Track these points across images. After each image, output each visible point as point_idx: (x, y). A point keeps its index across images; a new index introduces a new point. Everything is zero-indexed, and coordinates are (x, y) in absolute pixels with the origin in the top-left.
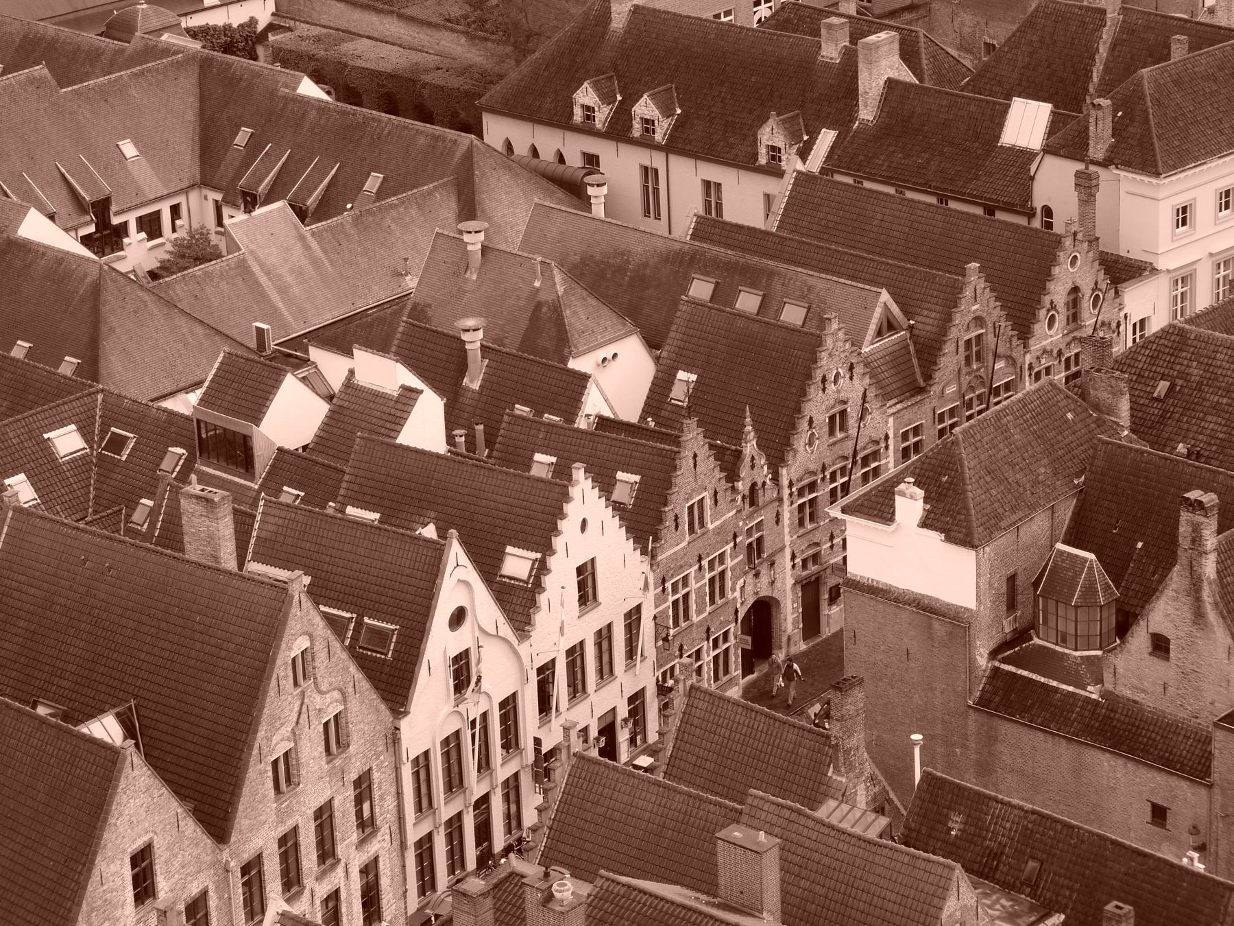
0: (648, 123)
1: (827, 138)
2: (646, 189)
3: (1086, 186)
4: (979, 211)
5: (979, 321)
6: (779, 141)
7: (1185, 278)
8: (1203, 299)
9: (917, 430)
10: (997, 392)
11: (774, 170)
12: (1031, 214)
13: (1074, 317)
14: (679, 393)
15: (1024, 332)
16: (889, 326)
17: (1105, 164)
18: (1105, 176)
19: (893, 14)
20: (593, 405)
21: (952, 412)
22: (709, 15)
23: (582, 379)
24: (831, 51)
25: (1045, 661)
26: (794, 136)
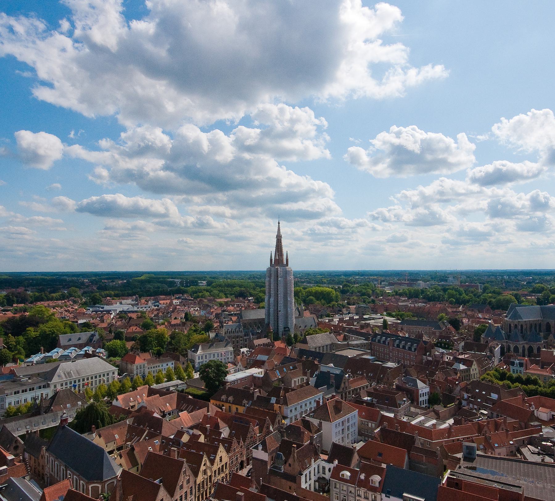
0: (230, 401)
7: (291, 418)
11: (244, 406)
13: (279, 424)
20: (222, 436)
23: (221, 432)
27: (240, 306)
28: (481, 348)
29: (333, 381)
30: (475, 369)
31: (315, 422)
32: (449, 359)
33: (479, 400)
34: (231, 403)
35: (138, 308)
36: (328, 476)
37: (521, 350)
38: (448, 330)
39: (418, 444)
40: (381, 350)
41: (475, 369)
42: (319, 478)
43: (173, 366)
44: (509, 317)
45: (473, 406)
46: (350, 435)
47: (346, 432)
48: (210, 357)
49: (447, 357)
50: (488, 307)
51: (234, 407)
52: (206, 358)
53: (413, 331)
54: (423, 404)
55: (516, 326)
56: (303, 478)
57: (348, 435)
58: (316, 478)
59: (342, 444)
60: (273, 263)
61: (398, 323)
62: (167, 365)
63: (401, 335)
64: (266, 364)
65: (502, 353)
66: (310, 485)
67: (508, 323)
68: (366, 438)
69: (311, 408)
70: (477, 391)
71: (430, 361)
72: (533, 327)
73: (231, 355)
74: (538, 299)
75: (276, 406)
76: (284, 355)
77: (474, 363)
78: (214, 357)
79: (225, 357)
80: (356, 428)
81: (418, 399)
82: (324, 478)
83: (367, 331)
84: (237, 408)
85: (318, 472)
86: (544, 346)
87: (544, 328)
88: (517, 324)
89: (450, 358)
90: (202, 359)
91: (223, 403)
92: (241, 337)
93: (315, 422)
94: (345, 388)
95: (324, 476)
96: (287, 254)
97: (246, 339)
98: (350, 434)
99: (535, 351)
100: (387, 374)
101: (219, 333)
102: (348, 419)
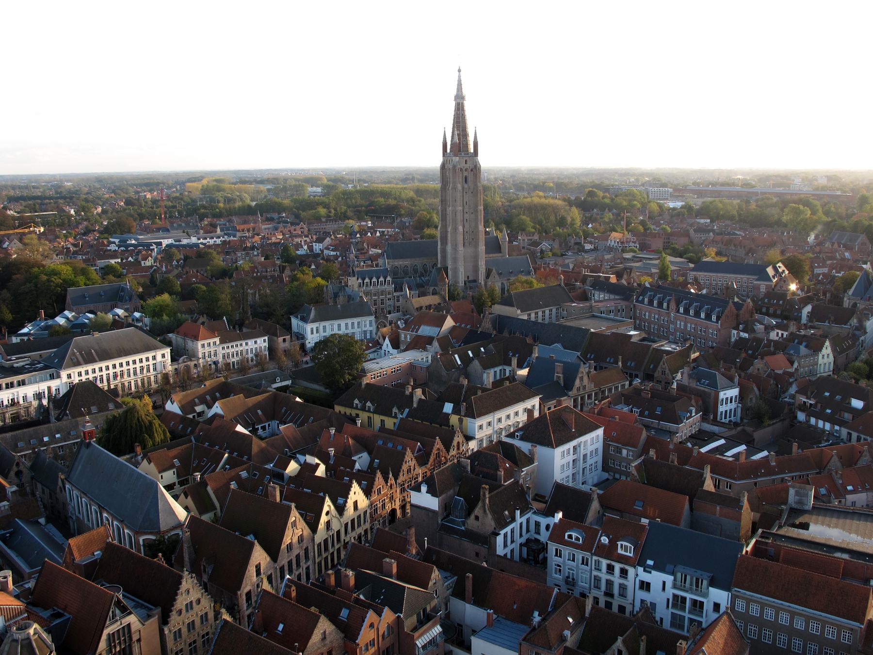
1: (407, 410)
3: (461, 421)
4: (438, 426)
5: (438, 449)
6: (397, 411)
7: (482, 440)
11: (396, 417)
12: (449, 427)
14: (375, 465)
15: (448, 451)
17: (465, 416)
18: (464, 419)
19: (421, 385)
20: (357, 466)
22: (382, 385)
23: (355, 461)
24: (407, 393)
25: (453, 522)
26: (400, 410)
27: (386, 233)
29: (559, 375)
30: (828, 354)
31: (525, 446)
32: (780, 335)
33: (829, 411)
34: (372, 412)
35: (199, 239)
36: (544, 536)
39: (709, 485)
42: (528, 540)
43: (266, 344)
45: (817, 423)
46: (587, 471)
47: (581, 465)
48: (332, 330)
49: (778, 333)
51: (377, 419)
52: (325, 331)
53: (717, 284)
56: (500, 539)
57: (583, 469)
58: (523, 540)
60: (448, 151)
62: (256, 342)
63: (692, 291)
64: (436, 344)
66: (512, 551)
68: (617, 476)
70: (827, 394)
71: (745, 339)
73: (370, 326)
75: (454, 419)
77: (827, 343)
78: (339, 329)
80: (599, 458)
82: (537, 541)
84: (382, 421)
85: (528, 531)
89: (782, 335)
90: (317, 332)
92: (389, 293)
93: (525, 446)
94: (581, 388)
95: (537, 537)
96: (476, 133)
97: (398, 297)
100: (661, 363)
101: (347, 286)
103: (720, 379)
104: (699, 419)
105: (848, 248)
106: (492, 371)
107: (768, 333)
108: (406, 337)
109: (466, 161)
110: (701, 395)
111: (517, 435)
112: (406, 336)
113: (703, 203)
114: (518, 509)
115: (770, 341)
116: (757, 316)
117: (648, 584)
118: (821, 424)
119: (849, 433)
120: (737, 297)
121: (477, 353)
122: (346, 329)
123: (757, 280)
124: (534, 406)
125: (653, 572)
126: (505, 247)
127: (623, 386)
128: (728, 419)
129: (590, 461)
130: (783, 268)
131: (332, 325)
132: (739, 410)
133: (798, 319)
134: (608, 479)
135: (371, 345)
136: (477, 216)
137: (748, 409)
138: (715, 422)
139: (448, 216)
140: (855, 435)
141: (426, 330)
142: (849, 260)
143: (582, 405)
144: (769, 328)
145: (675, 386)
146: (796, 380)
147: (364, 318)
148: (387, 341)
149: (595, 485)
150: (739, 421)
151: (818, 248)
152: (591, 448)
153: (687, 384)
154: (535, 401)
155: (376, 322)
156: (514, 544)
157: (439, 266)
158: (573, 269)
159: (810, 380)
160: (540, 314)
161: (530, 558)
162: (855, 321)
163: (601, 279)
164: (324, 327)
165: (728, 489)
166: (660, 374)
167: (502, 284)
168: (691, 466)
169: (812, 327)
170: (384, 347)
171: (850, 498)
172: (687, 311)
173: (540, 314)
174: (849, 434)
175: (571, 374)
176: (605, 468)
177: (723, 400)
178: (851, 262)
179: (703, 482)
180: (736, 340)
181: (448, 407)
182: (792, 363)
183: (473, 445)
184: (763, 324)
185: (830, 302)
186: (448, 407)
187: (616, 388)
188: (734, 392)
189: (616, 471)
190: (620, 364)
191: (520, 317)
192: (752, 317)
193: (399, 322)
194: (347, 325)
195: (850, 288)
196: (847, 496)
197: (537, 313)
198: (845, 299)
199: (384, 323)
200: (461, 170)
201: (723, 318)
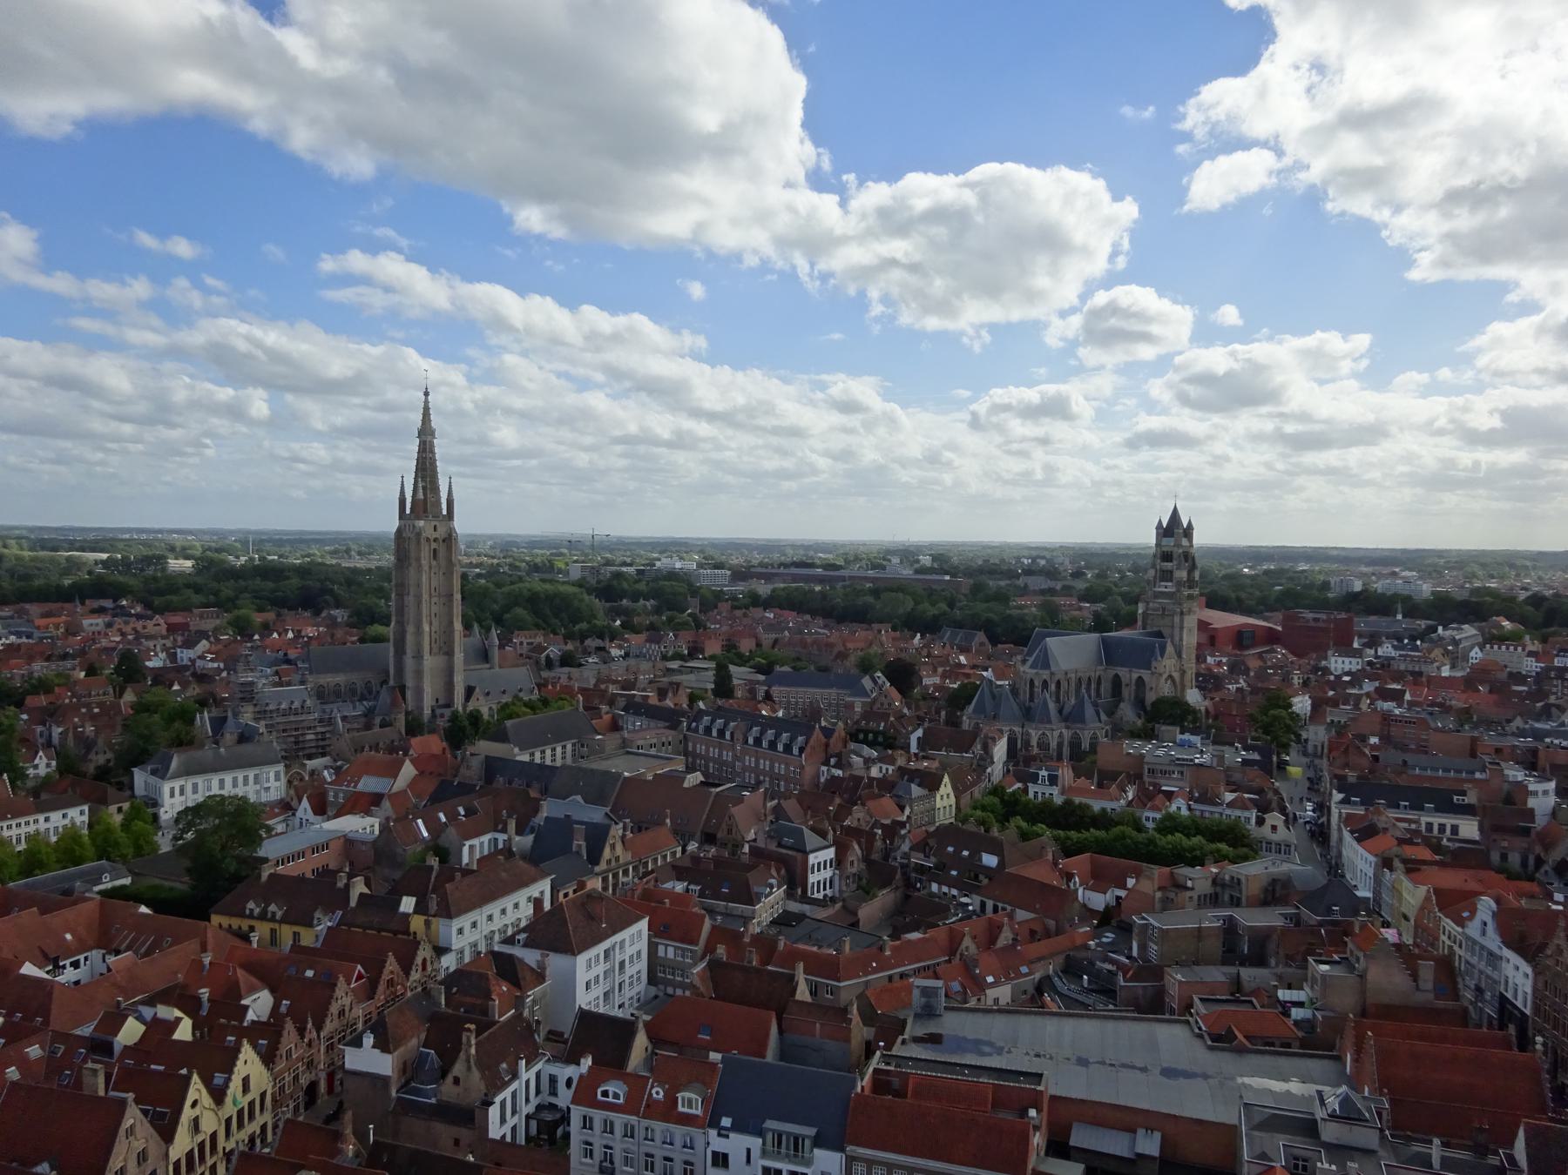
0: (274, 914)
2: (272, 936)
3: (427, 924)
5: (392, 972)
7: (462, 952)
8: (467, 960)
9: (370, 1013)
10: (398, 997)
12: (409, 934)
13: (424, 968)
14: (283, 1009)
16: (360, 977)
17: (434, 916)
18: (433, 920)
20: (251, 1016)
21: (382, 1006)
23: (246, 1008)
24: (340, 884)
25: (417, 1092)
28: (963, 742)
29: (580, 843)
30: (948, 795)
31: (530, 957)
32: (884, 771)
36: (564, 1098)
37: (1054, 744)
38: (886, 696)
39: (803, 993)
40: (714, 752)
41: (948, 795)
42: (539, 1108)
44: (1029, 664)
45: (940, 889)
48: (209, 789)
49: (881, 768)
50: (981, 636)
51: (286, 932)
53: (797, 703)
54: (818, 891)
55: (1045, 684)
56: (494, 1112)
57: (620, 984)
58: (531, 1109)
59: (601, 1010)
60: (408, 511)
61: (758, 682)
63: (764, 712)
64: (386, 804)
65: (1012, 752)
66: (514, 1129)
67: (1029, 677)
68: (670, 990)
69: (519, 920)
70: (950, 849)
71: (838, 777)
72: (1083, 686)
73: (277, 778)
74: (1097, 615)
75: (417, 923)
76: (440, 775)
77: (946, 779)
79: (258, 787)
80: (643, 965)
81: (806, 878)
82: (553, 1107)
83: (676, 705)
85: (538, 1092)
86: (1107, 731)
87: (1106, 687)
88: (1048, 680)
89: (887, 769)
91: (253, 923)
93: (530, 957)
94: (613, 860)
95: (553, 1100)
98: (627, 981)
99: (1085, 745)
100: (727, 818)
102: (623, 942)
103: (811, 839)
104: (783, 895)
105: (964, 650)
106: (475, 842)
107: (868, 768)
108: (336, 796)
109: (435, 527)
110: (782, 861)
111: (519, 940)
112: (335, 795)
113: (774, 591)
114: (522, 1059)
115: (871, 779)
116: (852, 746)
117: (725, 1156)
118: (945, 889)
119: (982, 901)
120: (826, 720)
121: (453, 816)
122: (234, 787)
123: (850, 696)
124: (542, 893)
125: (732, 1135)
126: (495, 654)
127: (674, 854)
128: (822, 893)
129: (630, 970)
130: (883, 678)
131: (210, 781)
132: (837, 878)
133: (906, 748)
134: (656, 997)
135: (277, 810)
136: (451, 608)
137: (848, 877)
138: (805, 899)
139: (406, 609)
140: (990, 904)
141: (368, 784)
142: (965, 665)
143: (615, 886)
144: (868, 762)
145: (746, 849)
146: (909, 832)
147: (266, 769)
148: (305, 803)
149: (637, 1008)
150: (837, 895)
151: (926, 650)
152: (630, 950)
153: (763, 846)
154: (543, 887)
155: (286, 773)
156: (516, 1118)
157: (392, 683)
158: (595, 685)
159: (926, 831)
160: (548, 752)
161: (542, 1136)
162: (979, 747)
163: (636, 700)
164: (195, 787)
165: (829, 996)
166: (725, 833)
167: (490, 708)
168: (776, 966)
169: (925, 758)
170: (300, 813)
171: (991, 993)
172: (758, 741)
173: (548, 752)
174: (983, 905)
175: (597, 838)
176: (652, 980)
177: (813, 865)
178: (967, 671)
179: (795, 989)
180: (826, 779)
181: (408, 904)
182: (902, 809)
183: (449, 962)
184: (861, 756)
185: (947, 723)
186: (408, 904)
187: (665, 857)
188: (830, 853)
189: (667, 983)
190: (668, 821)
191: (518, 758)
192: (845, 747)
193: (326, 772)
194: (235, 781)
195: (970, 703)
196: (987, 991)
197: (543, 752)
198: (965, 718)
199: (299, 773)
200: (428, 540)
201: (808, 749)
